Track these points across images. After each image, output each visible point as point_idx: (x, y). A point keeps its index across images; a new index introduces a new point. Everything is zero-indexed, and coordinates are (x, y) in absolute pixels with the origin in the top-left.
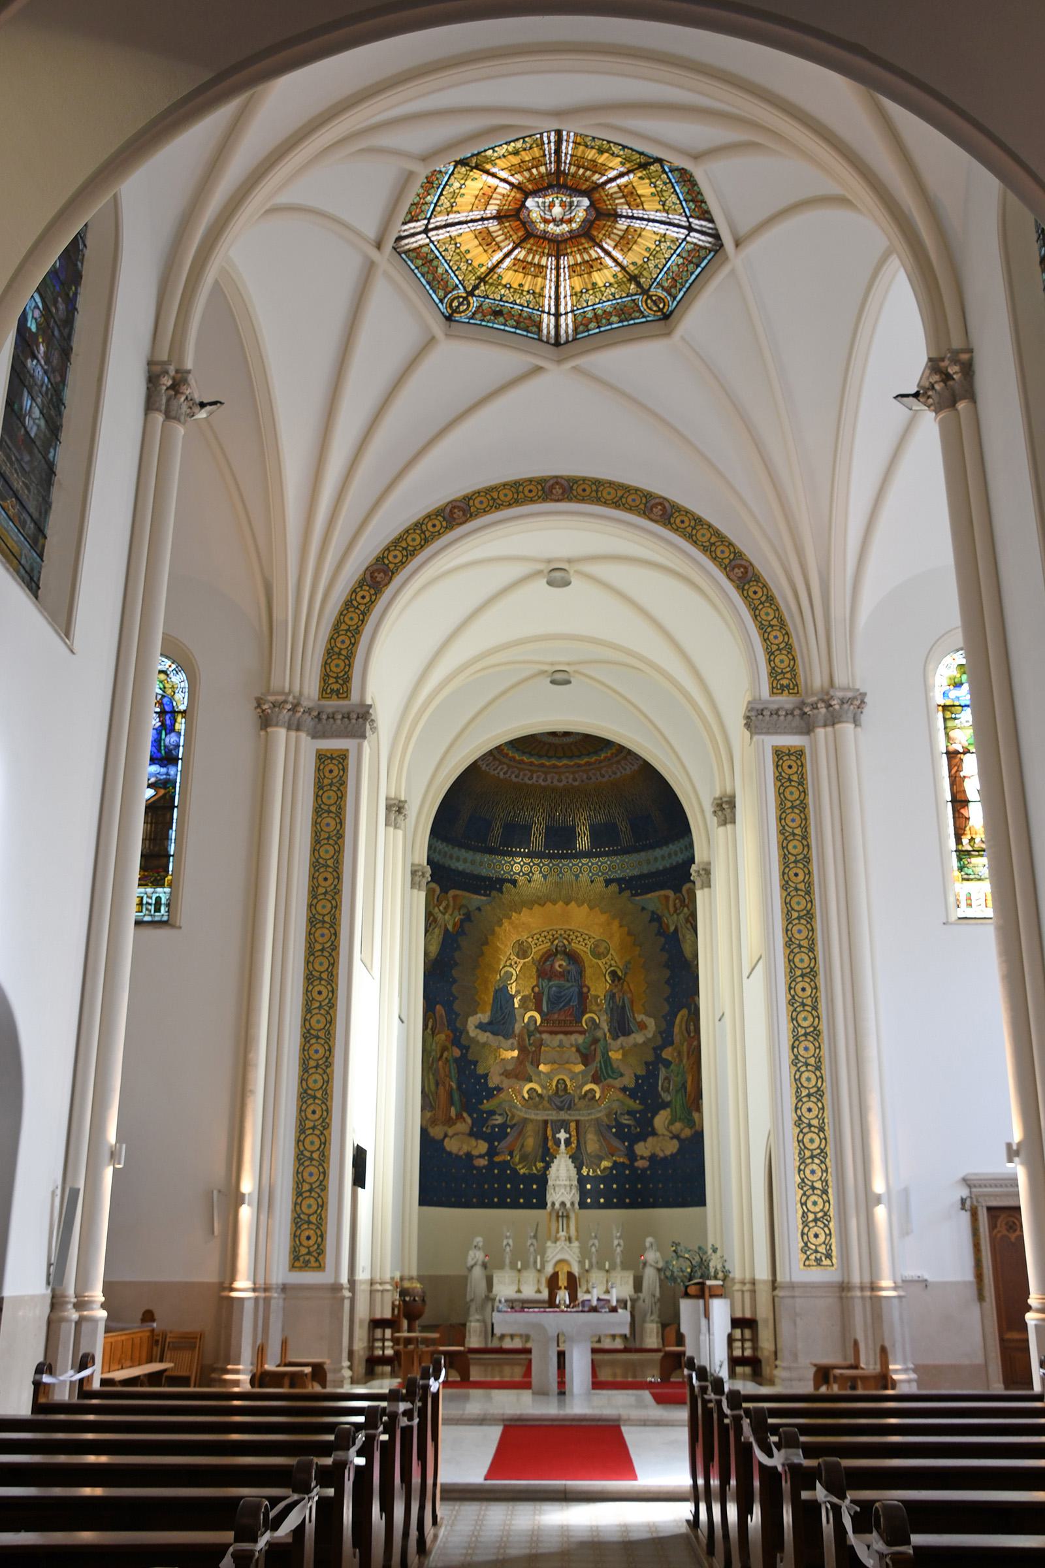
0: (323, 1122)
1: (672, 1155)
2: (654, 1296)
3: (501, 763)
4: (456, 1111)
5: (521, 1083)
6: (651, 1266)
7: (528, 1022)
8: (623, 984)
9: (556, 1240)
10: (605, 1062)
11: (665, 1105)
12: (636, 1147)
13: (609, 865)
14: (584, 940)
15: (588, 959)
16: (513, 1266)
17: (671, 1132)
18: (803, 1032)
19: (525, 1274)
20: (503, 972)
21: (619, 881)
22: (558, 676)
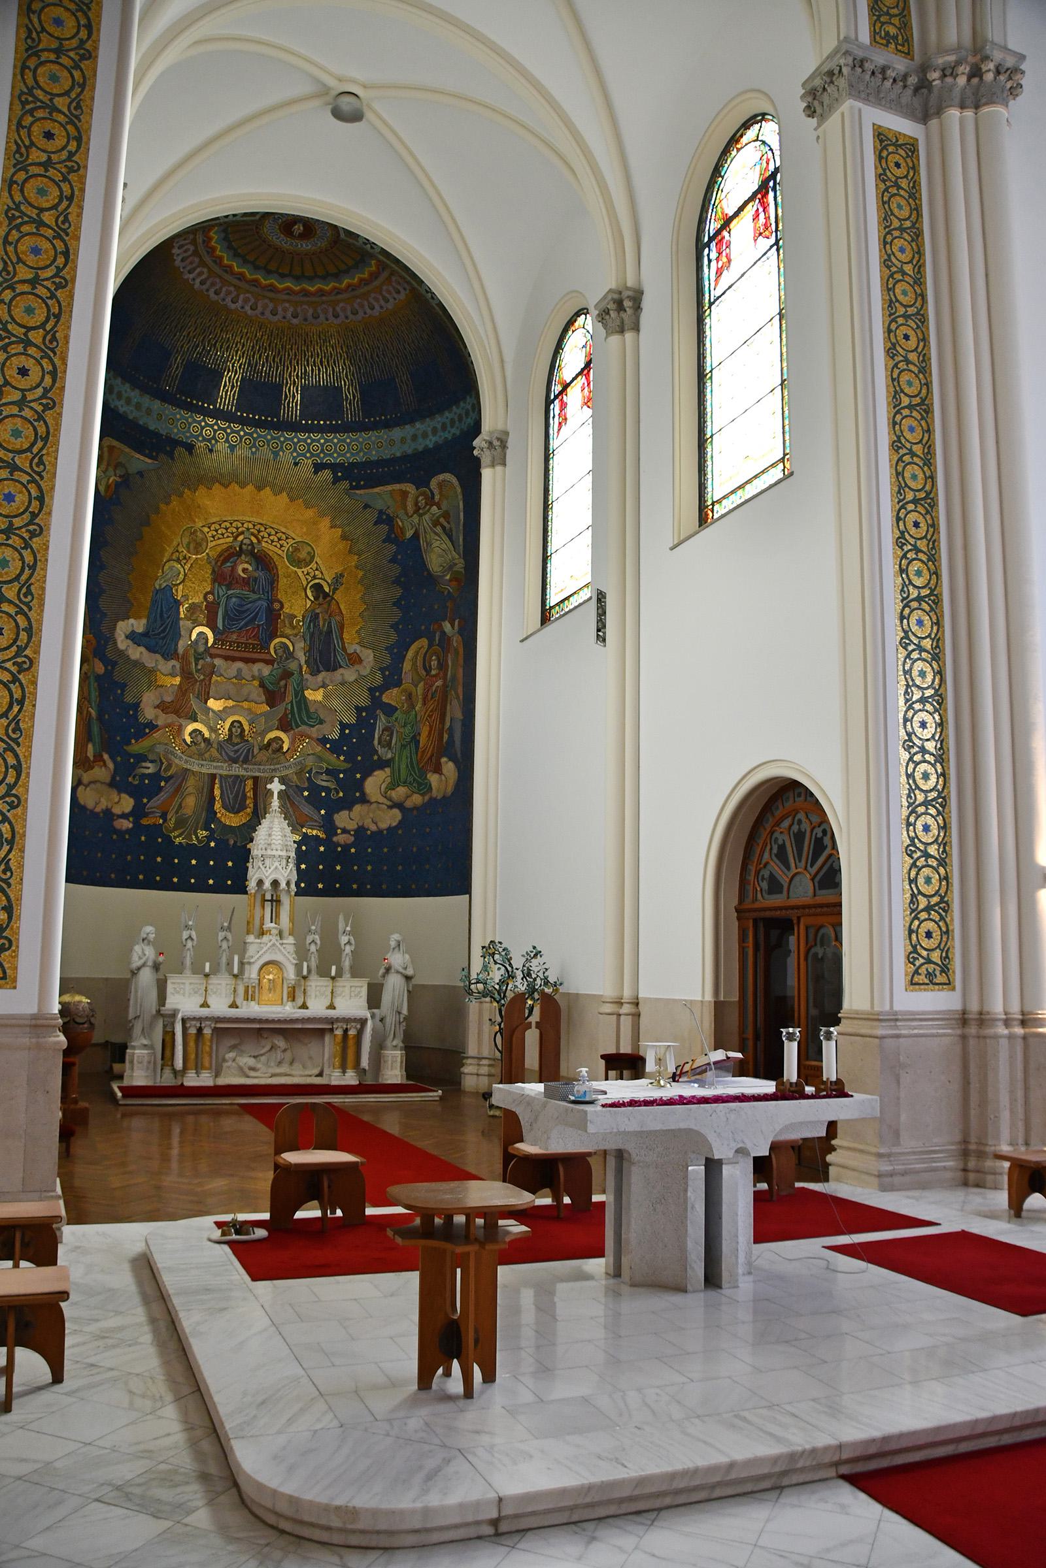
0: (17, 655)
1: (389, 829)
2: (399, 1013)
3: (203, 264)
4: (95, 749)
5: (181, 721)
6: (398, 972)
7: (197, 640)
8: (329, 603)
9: (262, 933)
10: (299, 703)
11: (382, 764)
12: (336, 816)
13: (322, 445)
14: (279, 539)
15: (284, 566)
16: (197, 969)
17: (390, 799)
18: (915, 595)
19: (214, 980)
20: (166, 567)
21: (333, 467)
22: (346, 103)
